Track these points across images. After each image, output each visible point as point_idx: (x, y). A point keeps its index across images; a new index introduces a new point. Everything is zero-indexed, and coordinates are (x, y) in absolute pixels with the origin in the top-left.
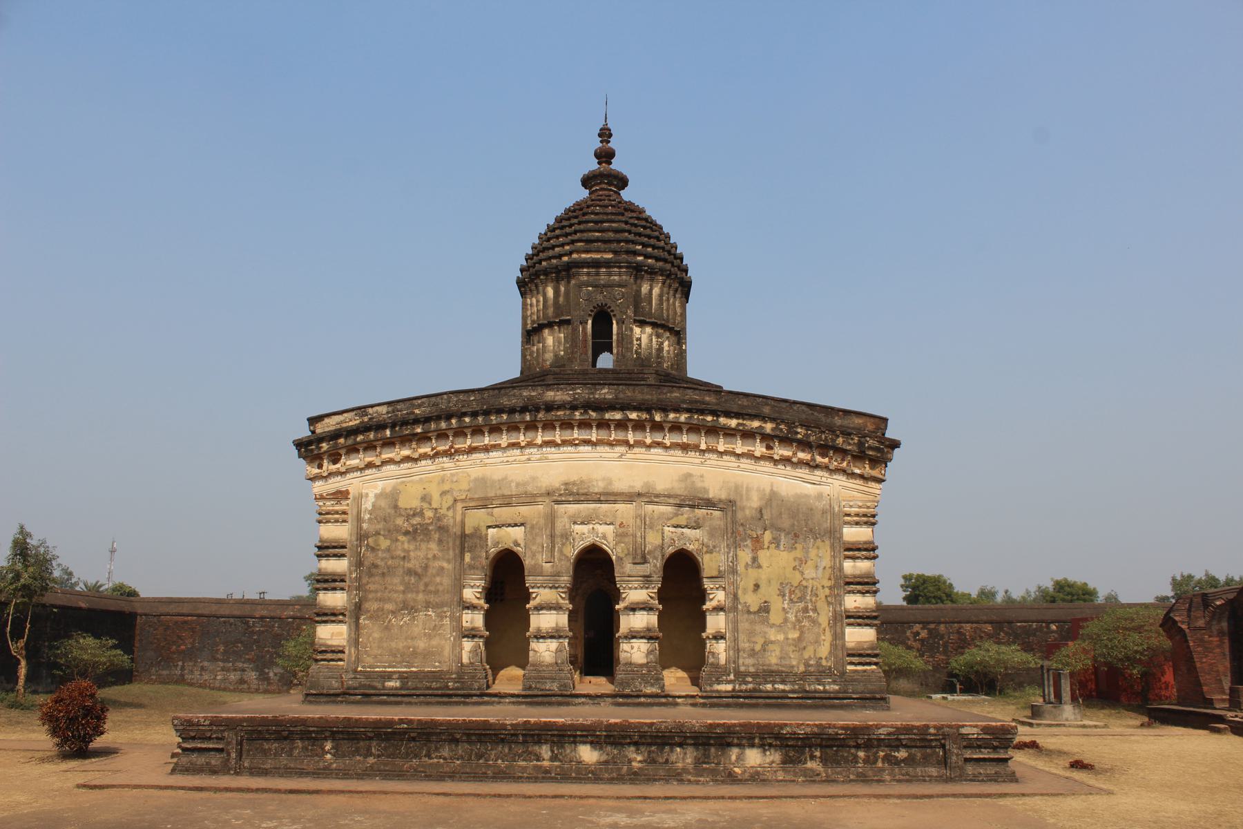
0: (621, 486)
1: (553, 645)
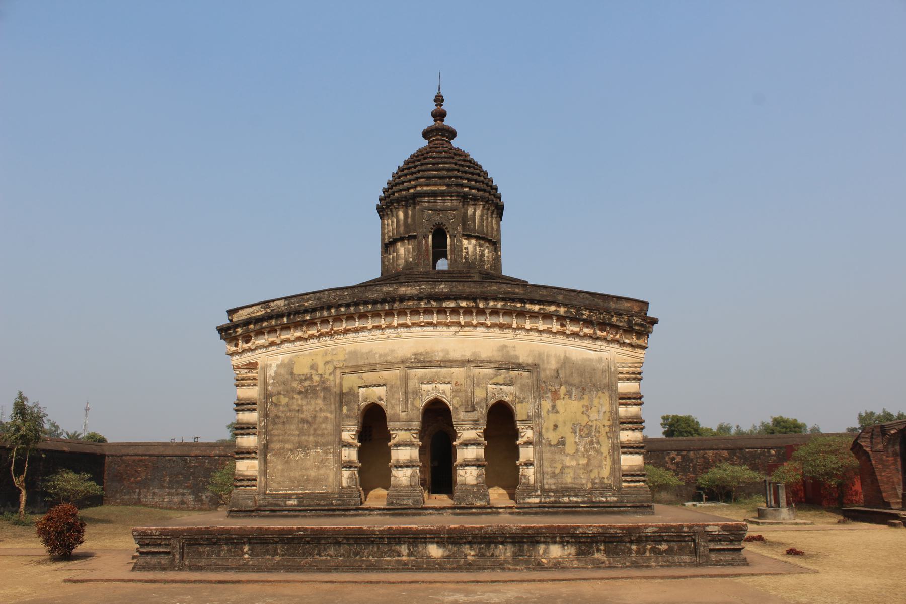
0: (455, 355)
1: (408, 472)
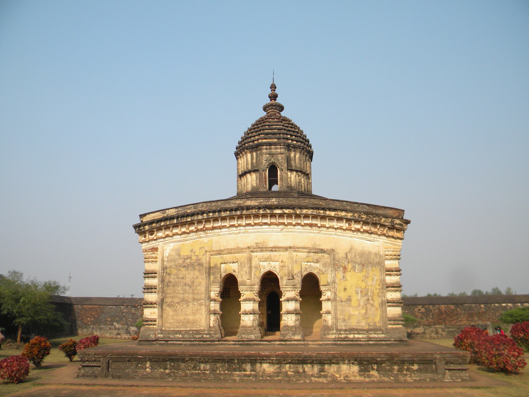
1: (252, 317)
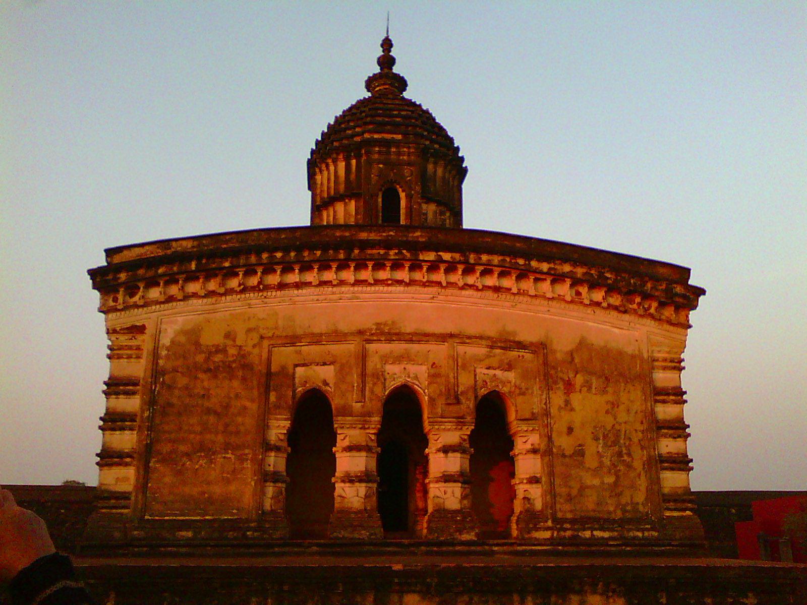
1: (362, 489)
